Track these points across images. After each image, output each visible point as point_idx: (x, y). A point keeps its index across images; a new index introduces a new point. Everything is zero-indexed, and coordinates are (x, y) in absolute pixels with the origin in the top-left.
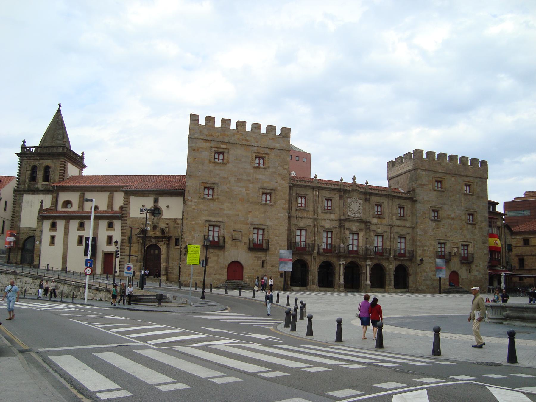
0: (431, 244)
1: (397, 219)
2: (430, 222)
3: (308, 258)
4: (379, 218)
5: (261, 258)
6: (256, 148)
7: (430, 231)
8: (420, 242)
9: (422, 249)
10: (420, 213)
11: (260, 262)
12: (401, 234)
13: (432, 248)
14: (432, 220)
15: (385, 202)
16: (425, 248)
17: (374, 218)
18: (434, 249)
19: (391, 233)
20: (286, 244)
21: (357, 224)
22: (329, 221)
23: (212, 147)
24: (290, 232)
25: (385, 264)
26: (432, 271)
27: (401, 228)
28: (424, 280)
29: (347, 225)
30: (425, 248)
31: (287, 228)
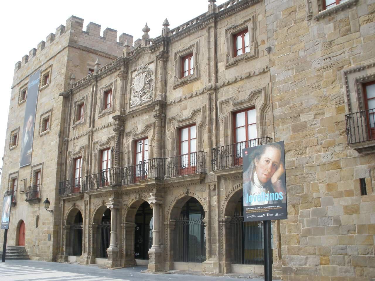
0: (325, 98)
1: (228, 67)
2: (314, 26)
3: (81, 206)
4: (184, 83)
5: (36, 211)
6: (44, 66)
7: (319, 52)
8: (284, 102)
9: (290, 124)
10: (276, 18)
11: (36, 218)
12: (241, 99)
13: (330, 112)
14: (318, 19)
15: (201, 40)
16: (303, 118)
17: (175, 88)
18: (339, 110)
19: (211, 109)
20: (55, 187)
21: (145, 117)
22: (106, 129)
23: (20, 88)
24: (61, 165)
25: (201, 196)
26: (340, 195)
27: (240, 84)
28: (308, 233)
29: (129, 126)
30: (303, 118)
31: (56, 161)
